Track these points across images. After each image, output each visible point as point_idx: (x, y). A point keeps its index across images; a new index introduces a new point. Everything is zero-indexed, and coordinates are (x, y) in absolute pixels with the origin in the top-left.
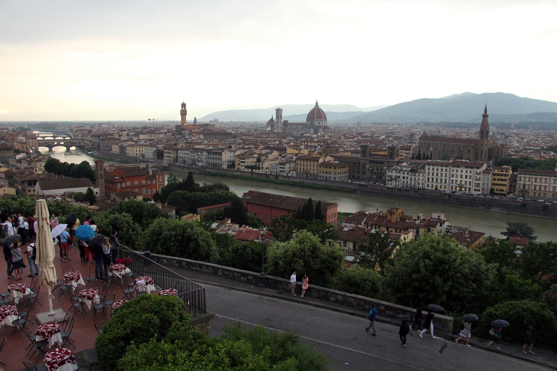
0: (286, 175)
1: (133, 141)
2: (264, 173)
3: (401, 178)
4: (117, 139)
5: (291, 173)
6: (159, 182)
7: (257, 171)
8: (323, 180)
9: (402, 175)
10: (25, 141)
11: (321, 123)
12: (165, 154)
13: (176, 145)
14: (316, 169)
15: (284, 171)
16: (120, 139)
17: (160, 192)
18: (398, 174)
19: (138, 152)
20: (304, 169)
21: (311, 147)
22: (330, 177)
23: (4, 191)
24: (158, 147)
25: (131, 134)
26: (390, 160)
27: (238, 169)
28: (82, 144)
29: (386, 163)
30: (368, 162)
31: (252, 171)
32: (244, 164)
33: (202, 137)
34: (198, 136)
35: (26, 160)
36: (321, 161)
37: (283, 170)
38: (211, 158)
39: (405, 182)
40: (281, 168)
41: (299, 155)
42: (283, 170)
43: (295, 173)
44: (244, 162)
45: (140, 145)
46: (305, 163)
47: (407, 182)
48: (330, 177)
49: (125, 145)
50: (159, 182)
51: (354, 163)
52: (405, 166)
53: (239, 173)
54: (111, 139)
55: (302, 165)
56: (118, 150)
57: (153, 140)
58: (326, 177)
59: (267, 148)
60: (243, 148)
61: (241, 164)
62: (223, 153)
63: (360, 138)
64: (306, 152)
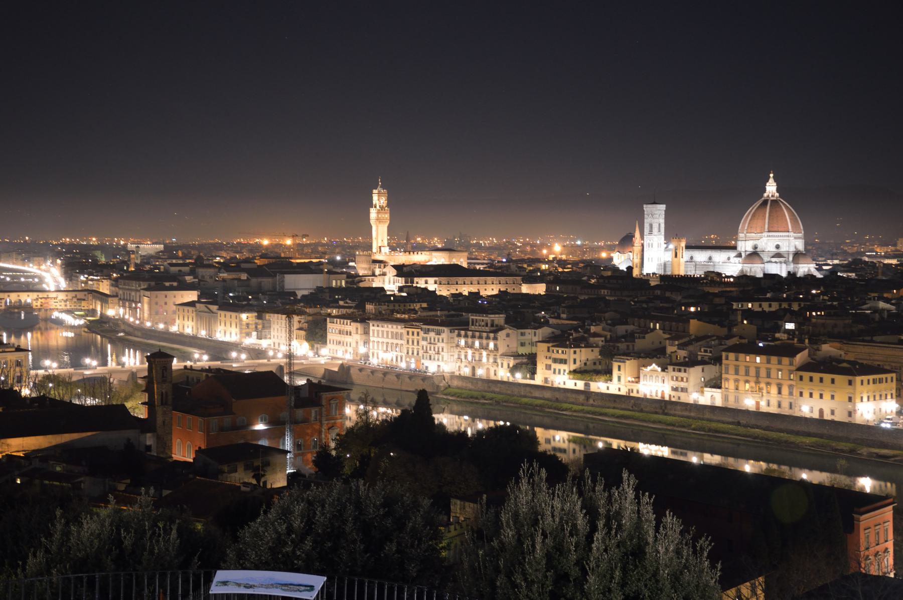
2: (623, 392)
12: (330, 337)
13: (361, 307)
27: (546, 380)
31: (587, 385)
32: (562, 367)
44: (564, 362)
53: (548, 395)
58: (821, 412)
61: (554, 366)
62: (502, 334)
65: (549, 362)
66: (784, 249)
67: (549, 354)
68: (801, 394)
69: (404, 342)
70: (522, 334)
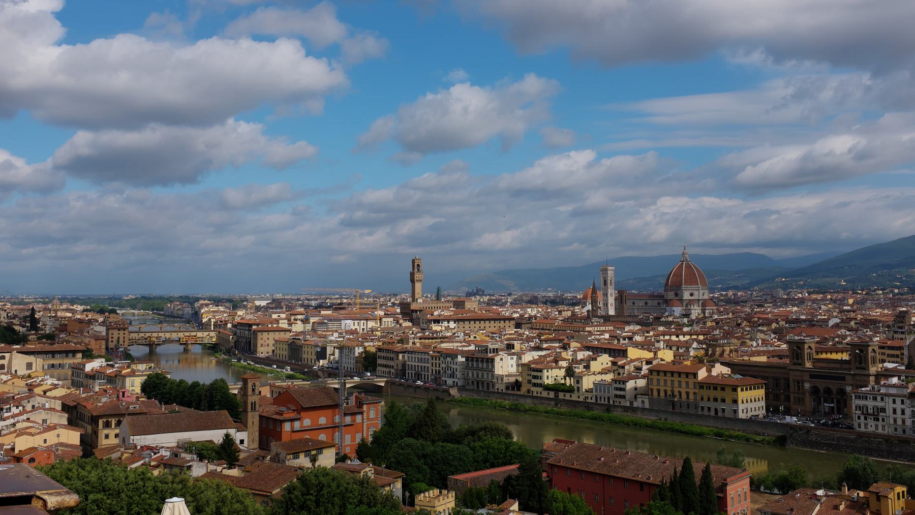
0: (628, 404)
2: (581, 399)
3: (889, 411)
4: (285, 331)
5: (640, 400)
6: (368, 419)
7: (568, 395)
8: (709, 416)
9: (889, 405)
11: (696, 293)
12: (379, 361)
14: (691, 391)
15: (623, 397)
16: (290, 331)
17: (370, 439)
18: (880, 404)
20: (666, 392)
21: (679, 345)
22: (723, 410)
24: (365, 348)
26: (858, 372)
27: (529, 391)
29: (848, 378)
30: (807, 377)
33: (452, 325)
34: (445, 324)
36: (702, 374)
37: (622, 393)
38: (472, 368)
39: (899, 422)
40: (617, 389)
41: (655, 362)
42: (622, 393)
43: (647, 401)
46: (669, 378)
47: (904, 421)
48: (723, 410)
50: (368, 419)
51: (776, 380)
52: (894, 386)
55: (662, 383)
56: (286, 353)
57: (354, 332)
58: (716, 410)
59: (588, 348)
60: (538, 348)
61: (534, 381)
62: (497, 359)
63: (782, 323)
64: (667, 356)
65: (530, 378)
66: (695, 297)
67: (529, 372)
68: (702, 399)
69: (430, 365)
70: (512, 359)
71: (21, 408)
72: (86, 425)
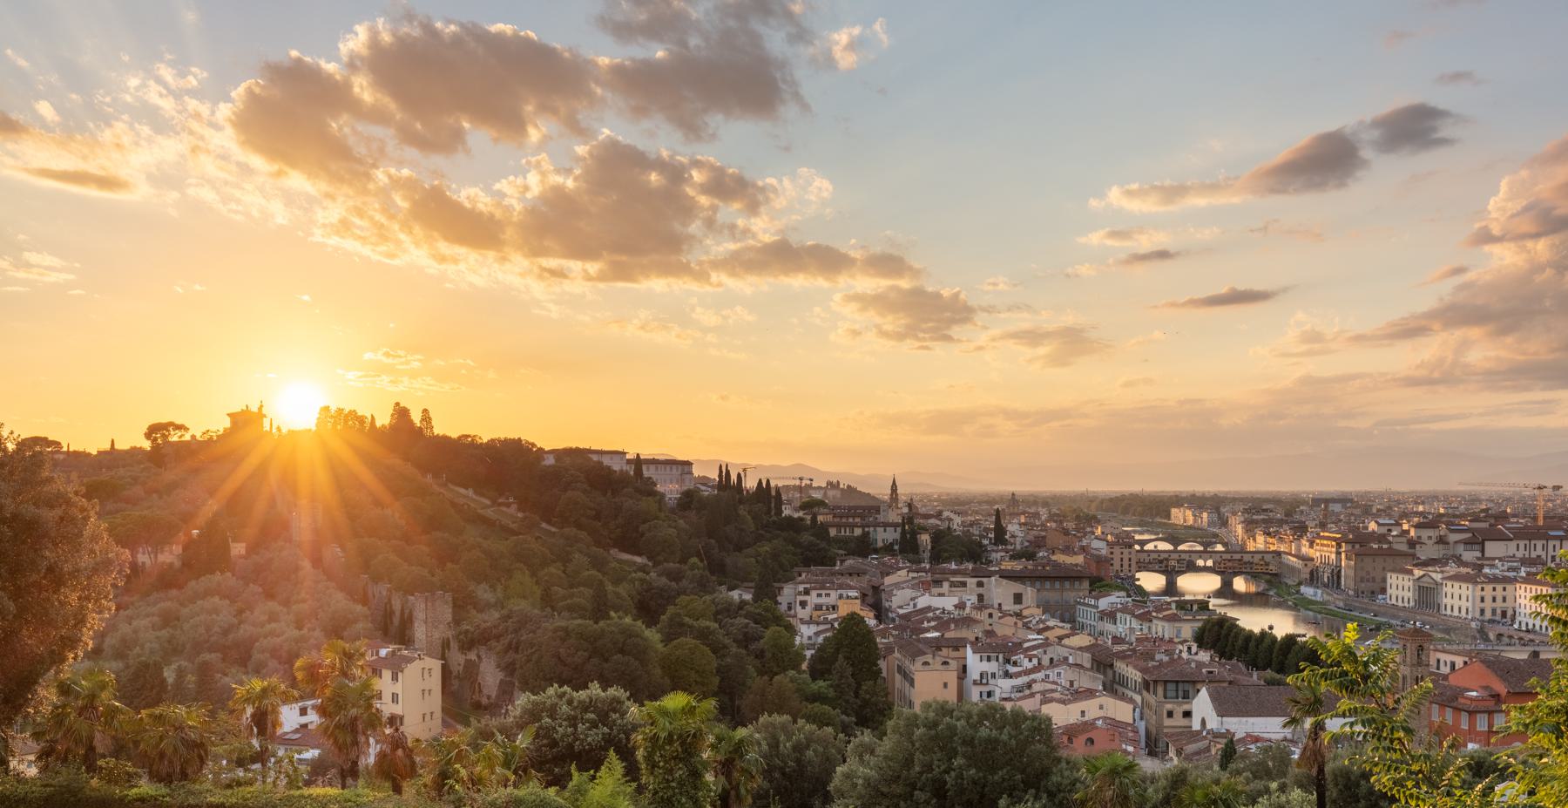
1: (1460, 561)
10: (1104, 552)
16: (1414, 556)
19: (1488, 605)
23: (1101, 707)
25: (1453, 537)
28: (1273, 568)
35: (1133, 615)
45: (1494, 580)
49: (1438, 577)
54: (1380, 553)
71: (1035, 661)
72: (1130, 694)
